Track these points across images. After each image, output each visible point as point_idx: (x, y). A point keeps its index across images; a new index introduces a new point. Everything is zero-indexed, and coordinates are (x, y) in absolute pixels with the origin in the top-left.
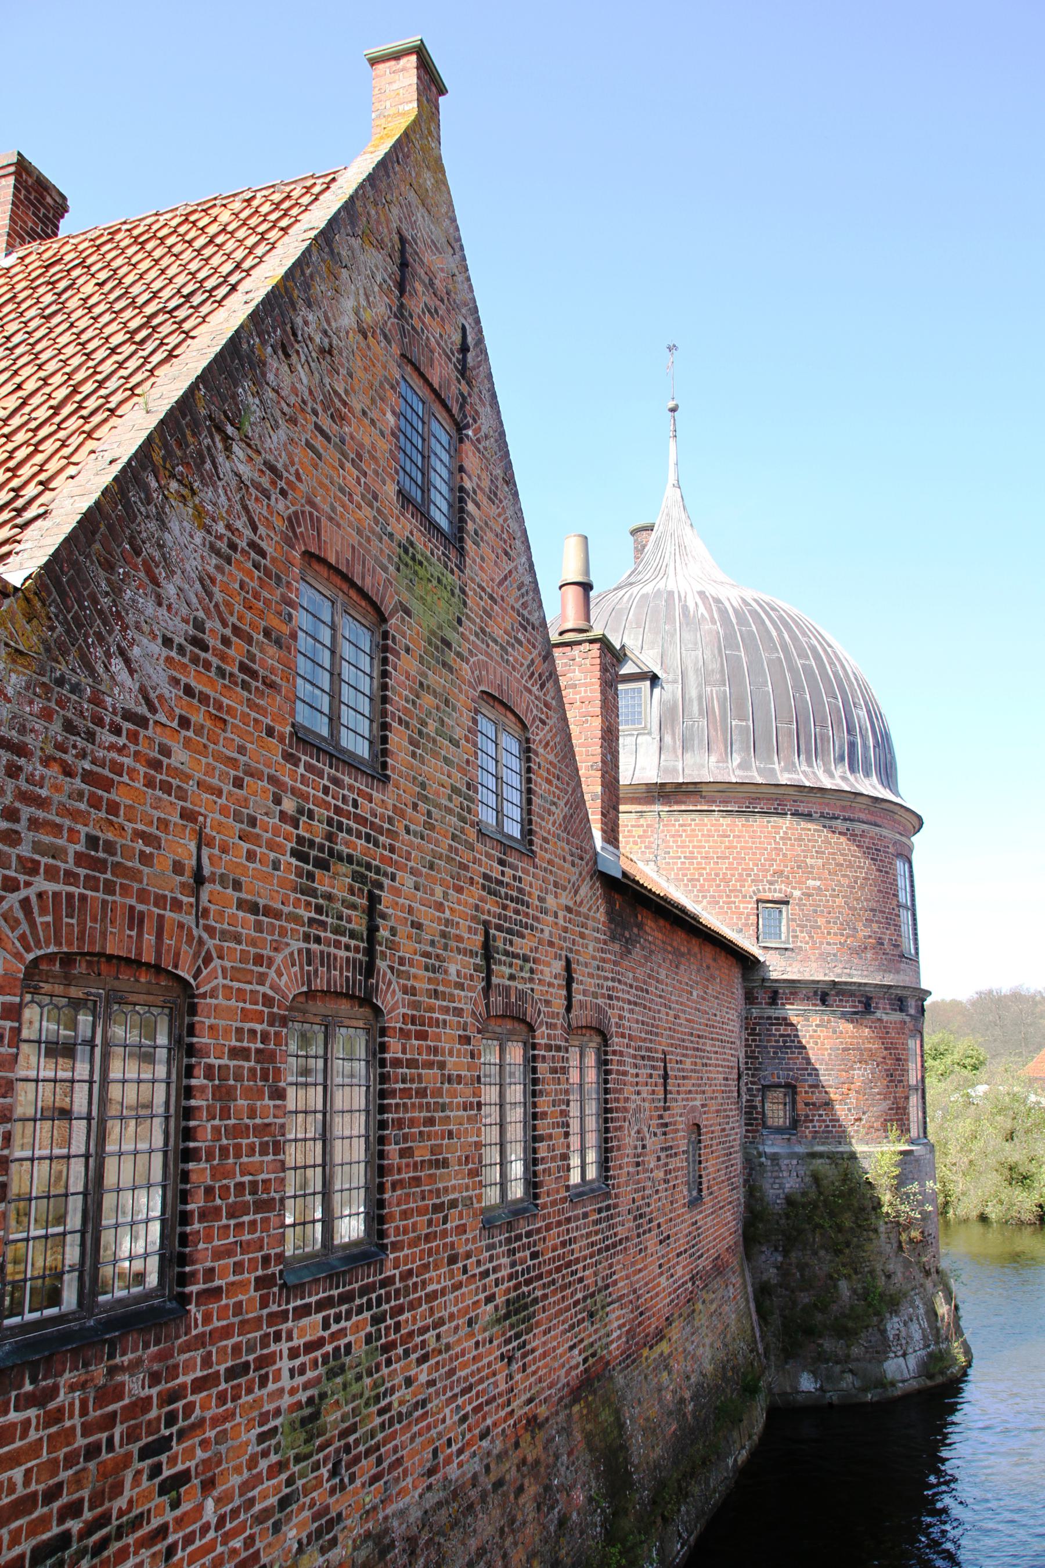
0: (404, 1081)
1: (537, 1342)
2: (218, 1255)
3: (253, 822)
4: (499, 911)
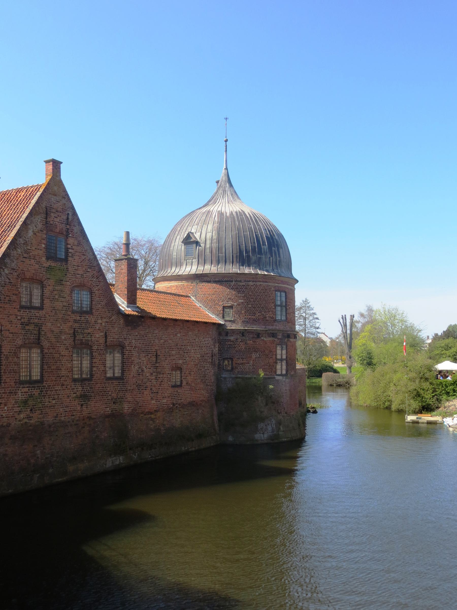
2: (6, 378)
3: (11, 321)
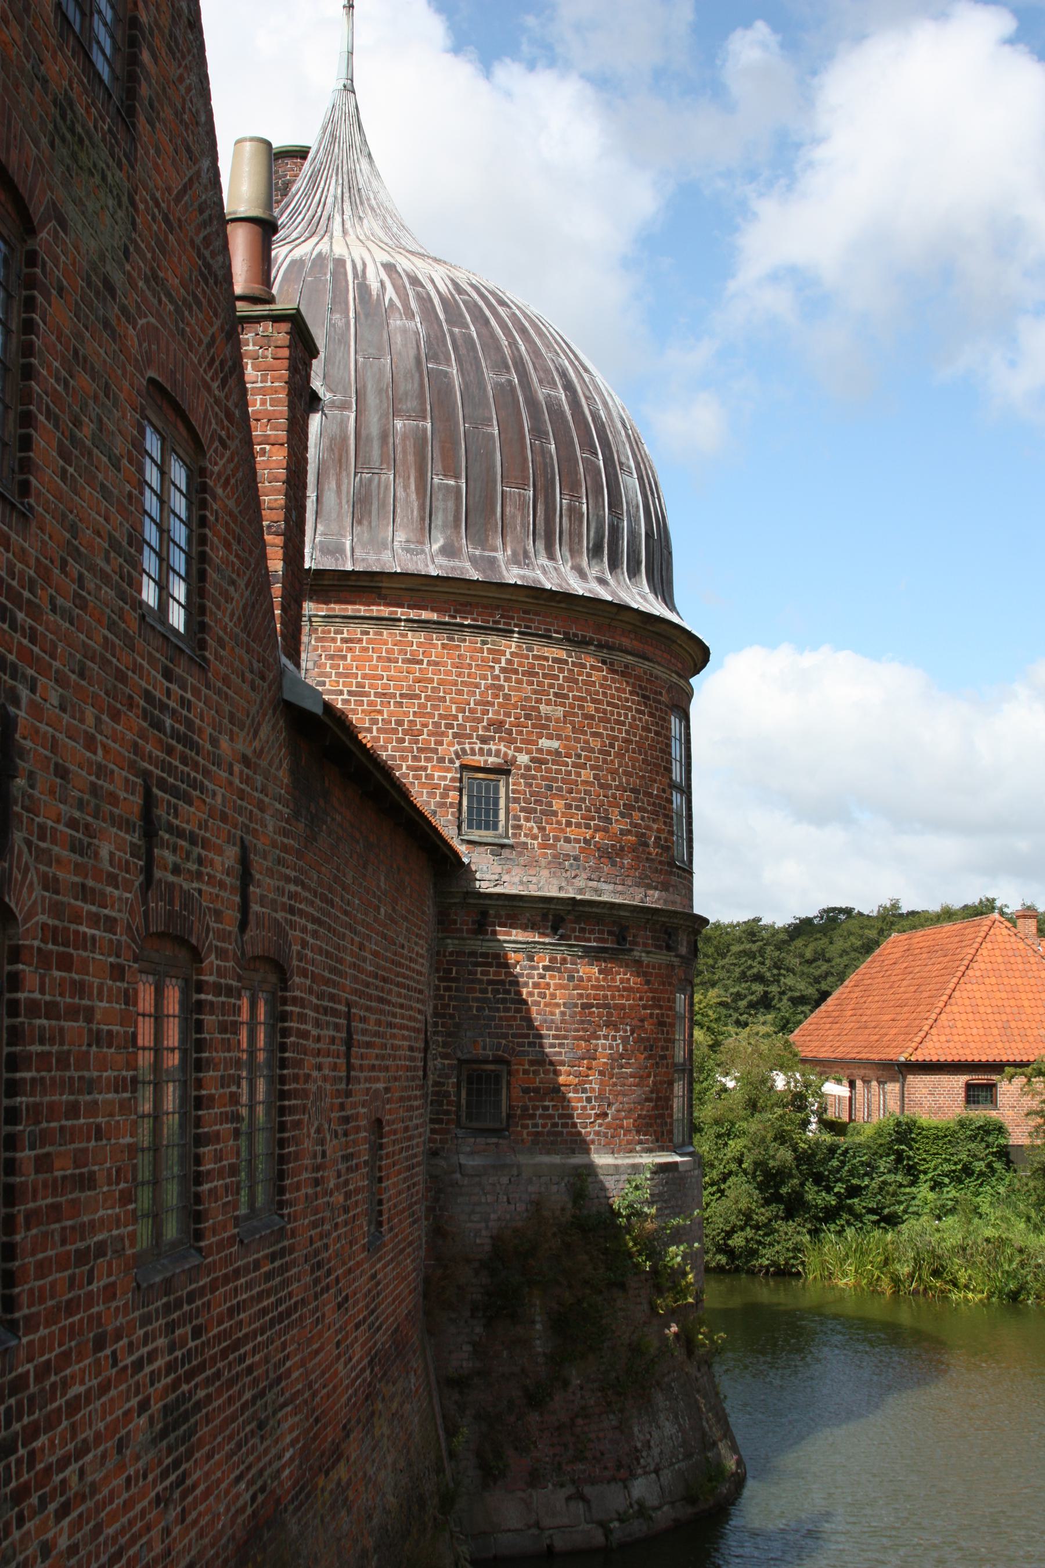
0: (42, 1042)
1: (199, 1473)
4: (162, 755)
